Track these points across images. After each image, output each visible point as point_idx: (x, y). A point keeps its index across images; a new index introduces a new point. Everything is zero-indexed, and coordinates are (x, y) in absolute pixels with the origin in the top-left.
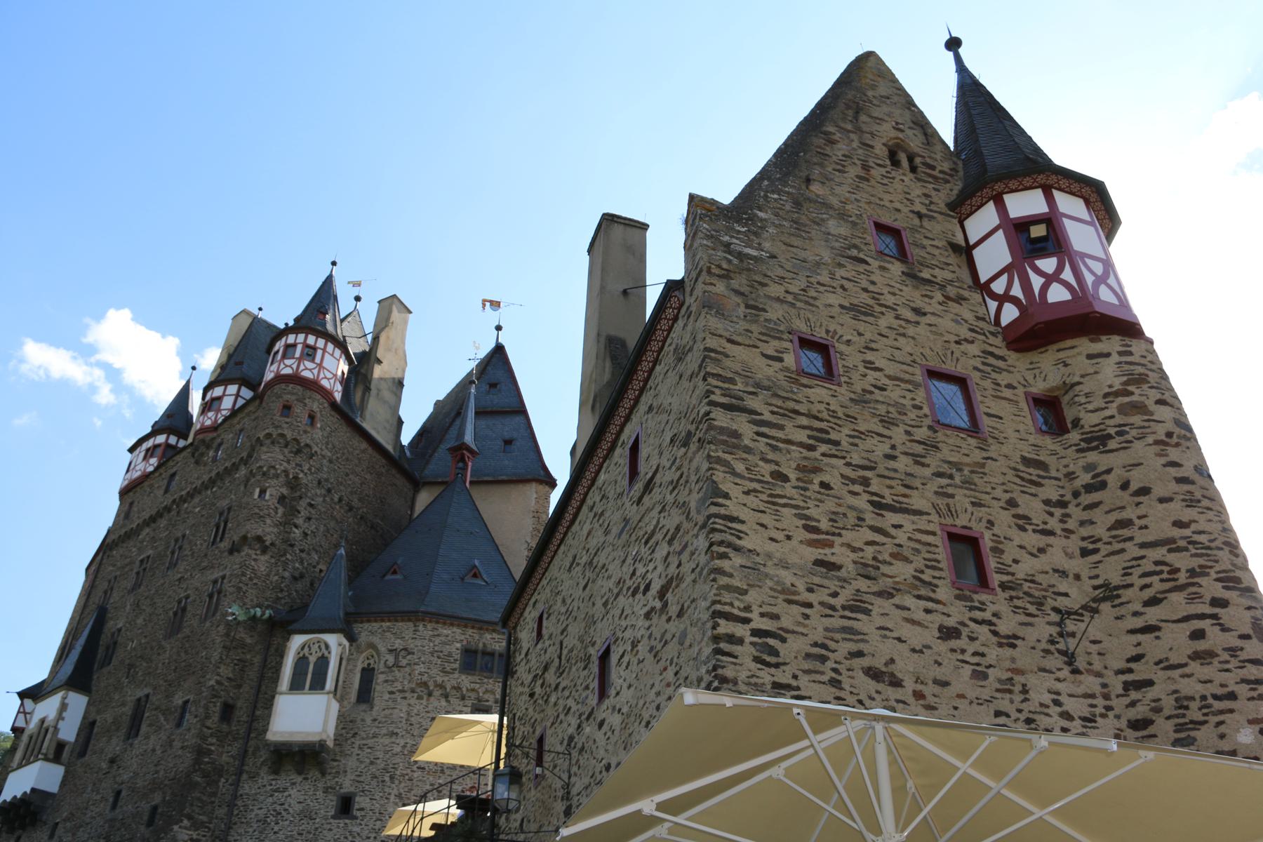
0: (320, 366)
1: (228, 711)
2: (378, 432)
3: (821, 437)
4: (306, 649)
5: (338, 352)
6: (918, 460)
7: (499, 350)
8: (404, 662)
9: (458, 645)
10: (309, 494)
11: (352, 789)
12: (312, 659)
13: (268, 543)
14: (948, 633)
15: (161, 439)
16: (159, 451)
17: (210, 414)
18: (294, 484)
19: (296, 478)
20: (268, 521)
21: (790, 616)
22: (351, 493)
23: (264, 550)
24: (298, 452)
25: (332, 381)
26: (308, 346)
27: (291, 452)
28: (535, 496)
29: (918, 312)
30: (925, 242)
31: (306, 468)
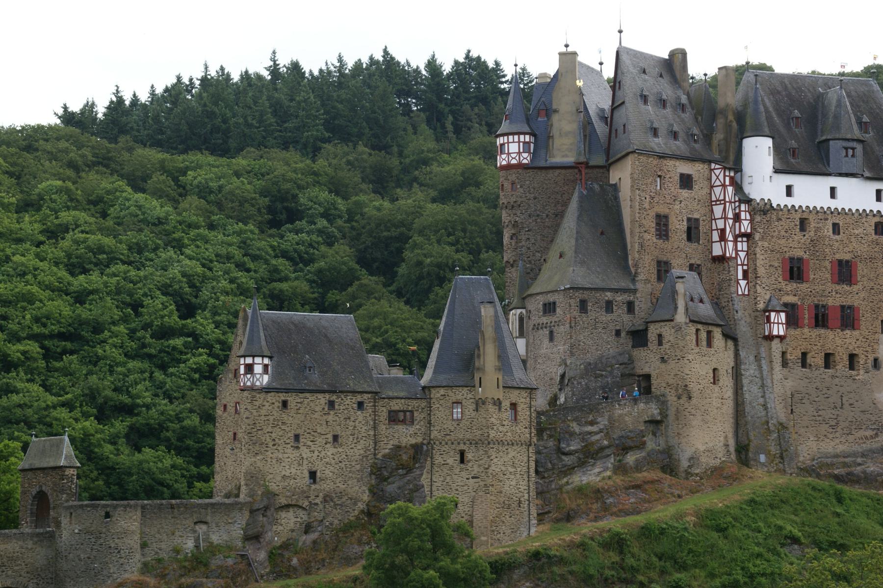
0: (509, 154)
2: (566, 156)
5: (516, 137)
7: (618, 53)
10: (525, 226)
18: (515, 225)
19: (516, 222)
22: (555, 206)
23: (512, 266)
24: (513, 207)
25: (517, 158)
31: (519, 215)
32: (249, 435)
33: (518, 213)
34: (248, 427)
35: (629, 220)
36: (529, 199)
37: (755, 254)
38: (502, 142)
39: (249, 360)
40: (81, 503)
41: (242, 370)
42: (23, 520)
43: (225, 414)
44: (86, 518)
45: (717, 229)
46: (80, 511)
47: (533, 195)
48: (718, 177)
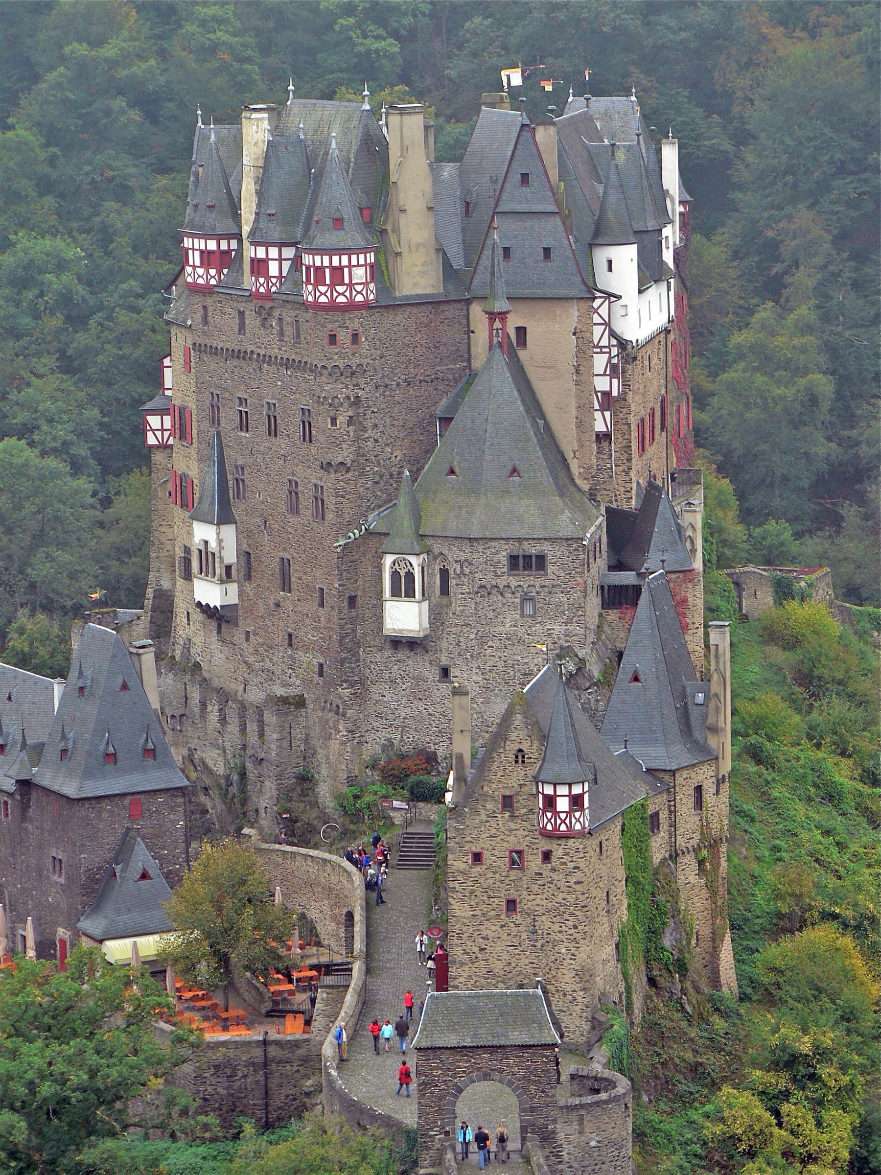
0: (351, 285)
1: (352, 601)
3: (477, 882)
4: (397, 566)
6: (502, 882)
8: (467, 571)
9: (505, 553)
10: (371, 403)
11: (447, 663)
12: (402, 574)
13: (349, 465)
14: (502, 926)
15: (212, 245)
16: (215, 259)
17: (262, 280)
20: (344, 446)
21: (465, 929)
23: (348, 470)
24: (353, 373)
26: (335, 268)
27: (347, 377)
28: (577, 314)
29: (511, 831)
30: (520, 798)
32: (585, 909)
33: (362, 381)
34: (582, 897)
35: (573, 403)
36: (375, 359)
37: (629, 425)
38: (336, 262)
39: (577, 790)
40: (596, 1098)
41: (563, 804)
42: (432, 1129)
43: (477, 869)
44: (607, 1120)
45: (596, 392)
46: (598, 1111)
47: (379, 352)
48: (596, 311)
